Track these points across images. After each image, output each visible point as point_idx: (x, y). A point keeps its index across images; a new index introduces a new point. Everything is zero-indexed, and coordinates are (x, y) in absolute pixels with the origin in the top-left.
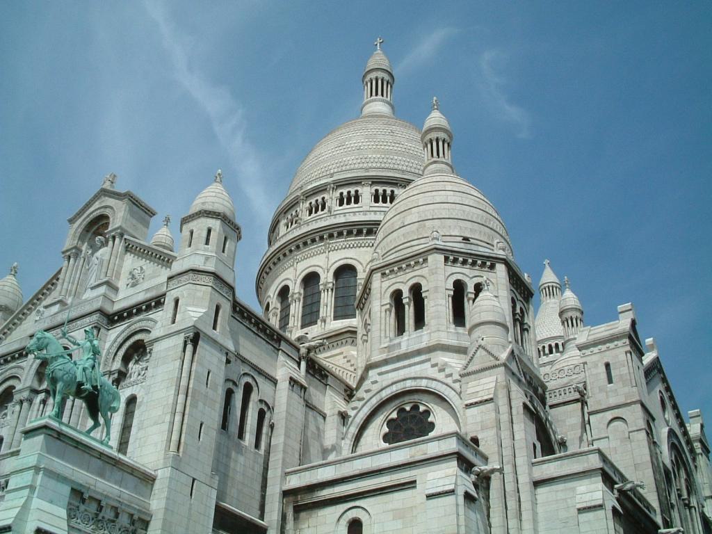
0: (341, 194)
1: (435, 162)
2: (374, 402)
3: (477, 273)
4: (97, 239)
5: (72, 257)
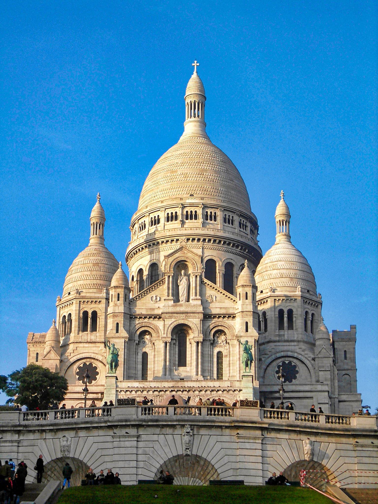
0: (207, 212)
1: (285, 235)
2: (274, 357)
3: (313, 309)
4: (183, 272)
5: (171, 277)
